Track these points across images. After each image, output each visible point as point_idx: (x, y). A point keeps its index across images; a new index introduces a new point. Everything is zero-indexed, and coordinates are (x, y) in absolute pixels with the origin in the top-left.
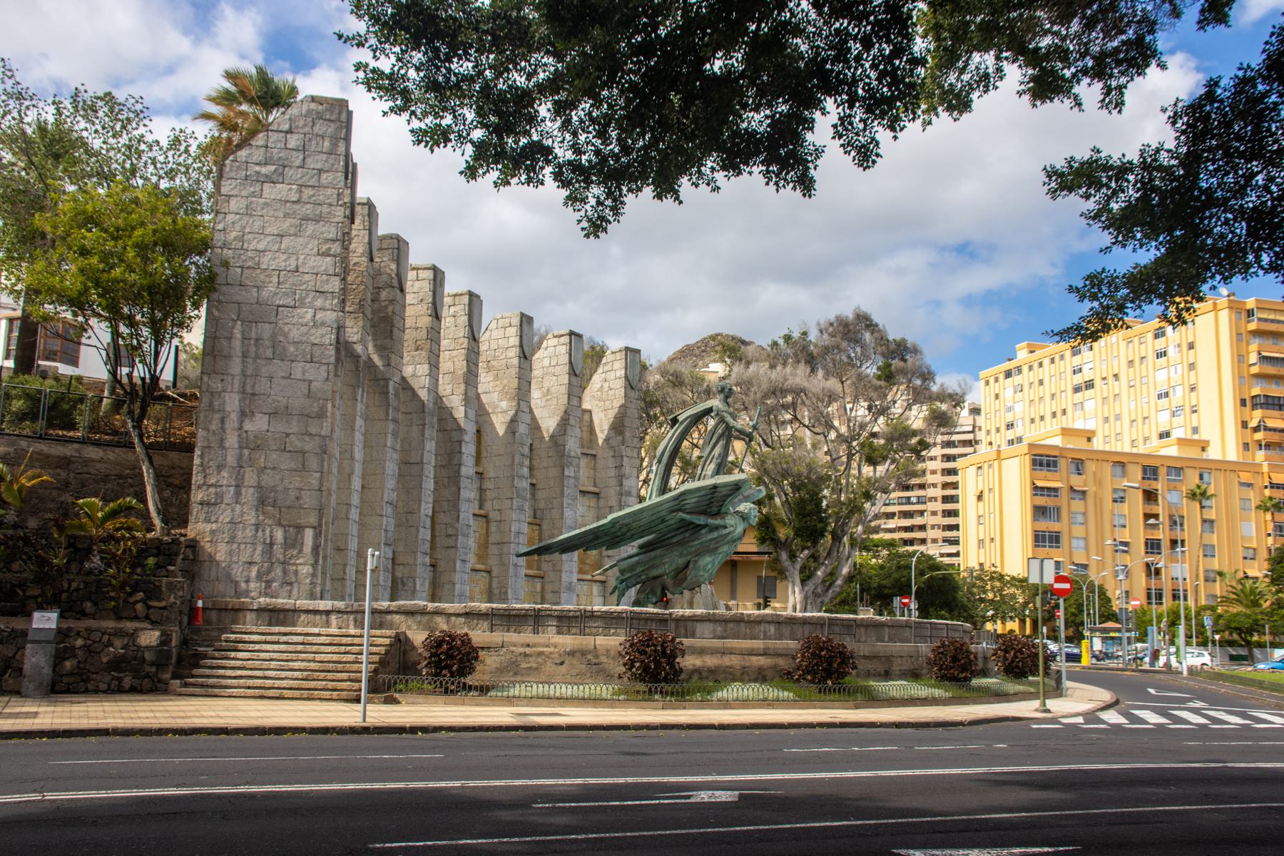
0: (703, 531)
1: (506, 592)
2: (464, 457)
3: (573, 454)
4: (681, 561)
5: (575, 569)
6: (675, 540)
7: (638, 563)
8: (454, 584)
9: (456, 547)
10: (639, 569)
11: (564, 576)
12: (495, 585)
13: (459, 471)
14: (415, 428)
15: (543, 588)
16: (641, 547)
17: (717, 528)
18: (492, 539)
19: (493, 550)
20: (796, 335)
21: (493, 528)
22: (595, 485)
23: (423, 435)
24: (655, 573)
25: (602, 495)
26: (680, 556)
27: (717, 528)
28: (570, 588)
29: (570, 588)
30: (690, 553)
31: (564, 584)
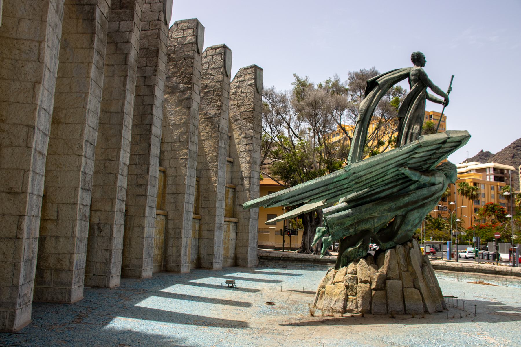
0: (412, 187)
1: (181, 232)
2: (155, 118)
3: (224, 131)
4: (390, 217)
5: (223, 215)
6: (383, 194)
7: (347, 216)
8: (143, 228)
9: (145, 196)
10: (348, 222)
11: (217, 219)
12: (170, 226)
13: (150, 130)
14: (117, 79)
15: (200, 227)
16: (348, 201)
17: (424, 186)
18: (169, 190)
19: (169, 198)
20: (324, 85)
21: (170, 181)
22: (230, 156)
23: (124, 85)
24: (364, 227)
25: (235, 163)
26: (390, 210)
27: (424, 186)
28: (220, 228)
29: (220, 228)
30: (400, 208)
31: (217, 225)
